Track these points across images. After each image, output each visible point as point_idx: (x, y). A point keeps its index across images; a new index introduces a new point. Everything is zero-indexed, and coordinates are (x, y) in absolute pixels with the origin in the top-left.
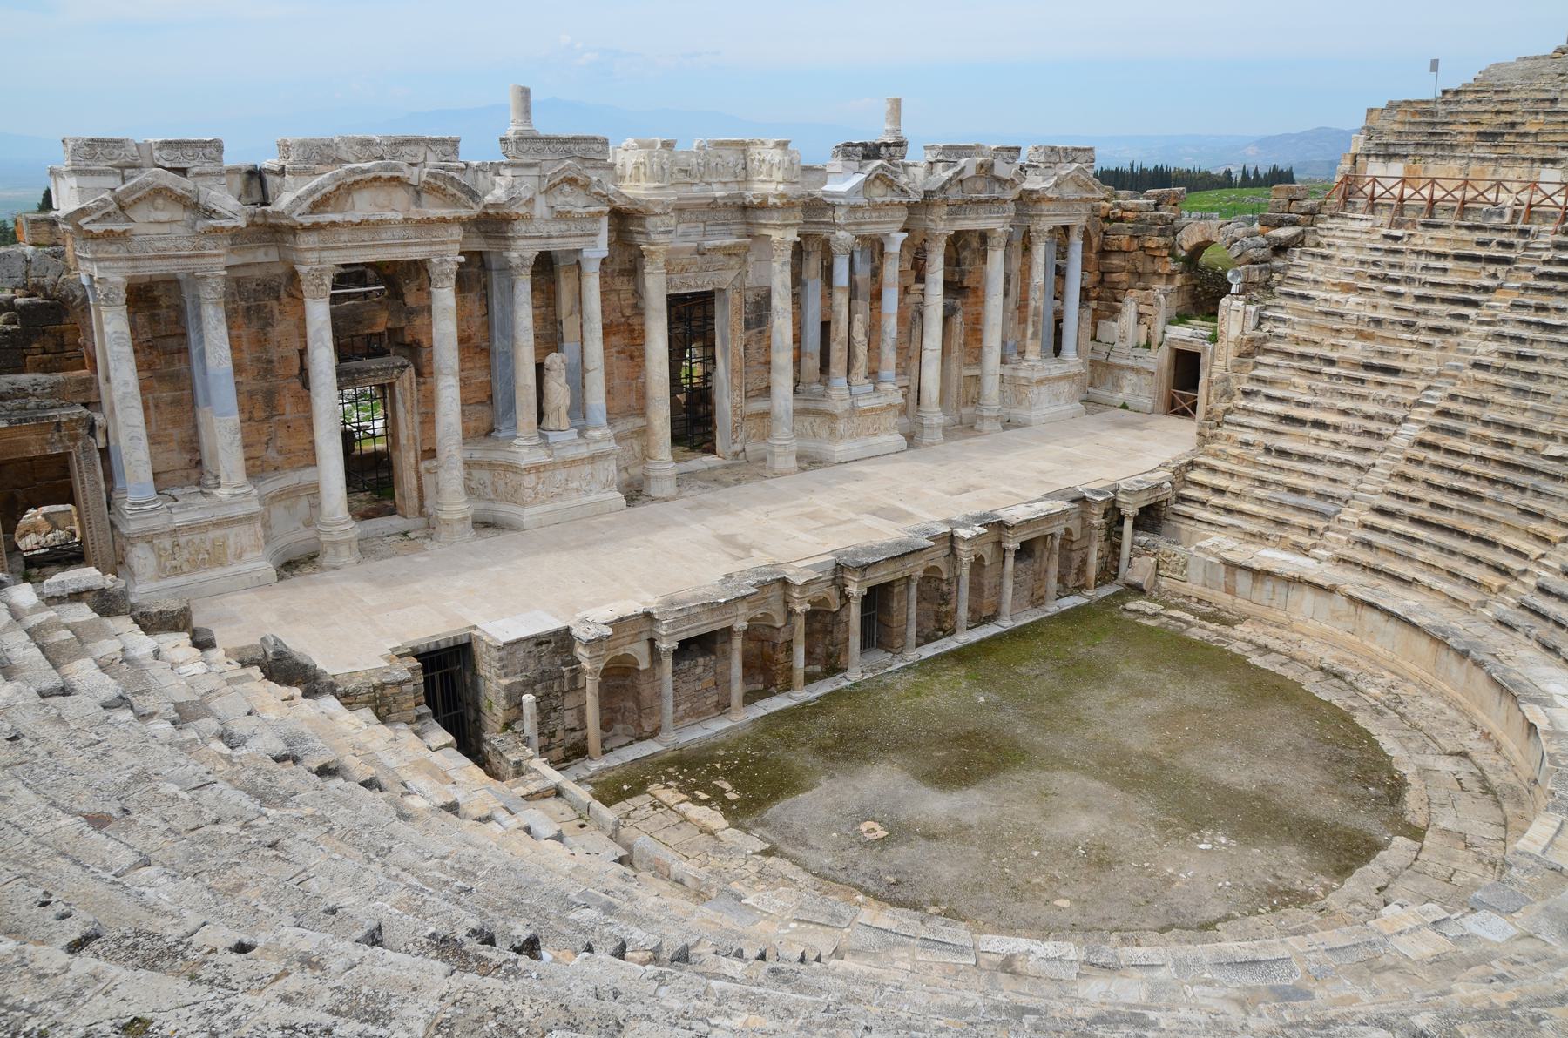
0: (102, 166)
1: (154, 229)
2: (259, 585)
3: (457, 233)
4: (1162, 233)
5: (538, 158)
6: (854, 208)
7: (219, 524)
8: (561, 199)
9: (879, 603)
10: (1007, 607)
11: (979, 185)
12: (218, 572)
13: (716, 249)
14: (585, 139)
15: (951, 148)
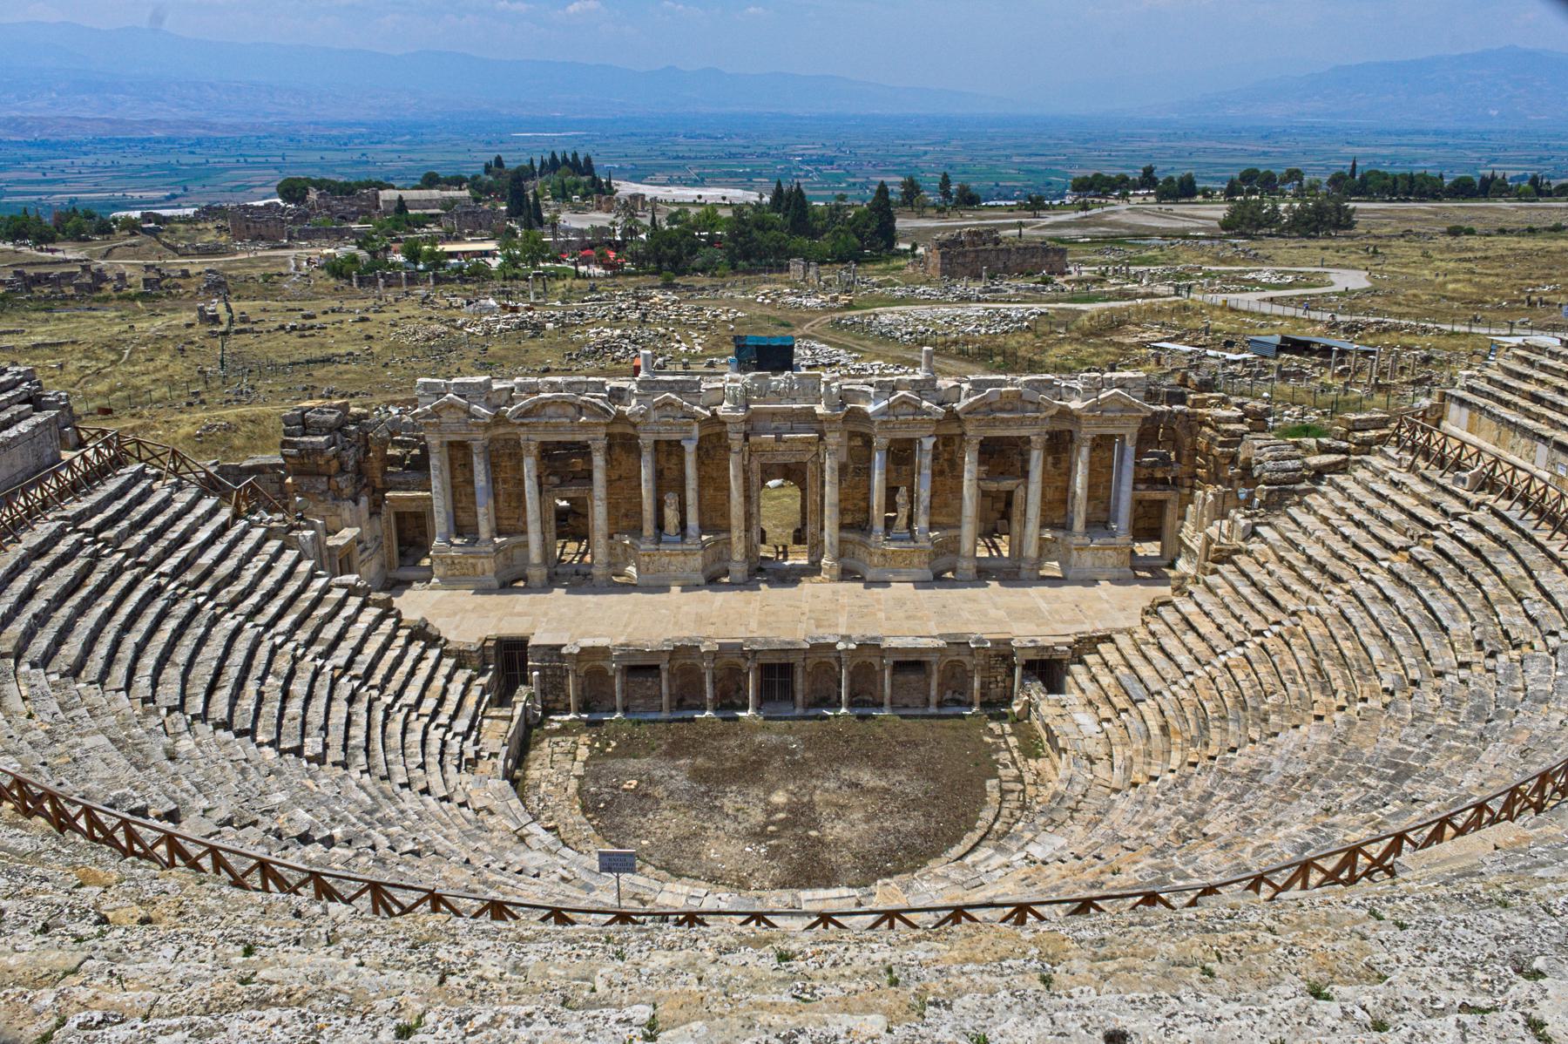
4: (1222, 444)
9: (779, 676)
10: (886, 701)
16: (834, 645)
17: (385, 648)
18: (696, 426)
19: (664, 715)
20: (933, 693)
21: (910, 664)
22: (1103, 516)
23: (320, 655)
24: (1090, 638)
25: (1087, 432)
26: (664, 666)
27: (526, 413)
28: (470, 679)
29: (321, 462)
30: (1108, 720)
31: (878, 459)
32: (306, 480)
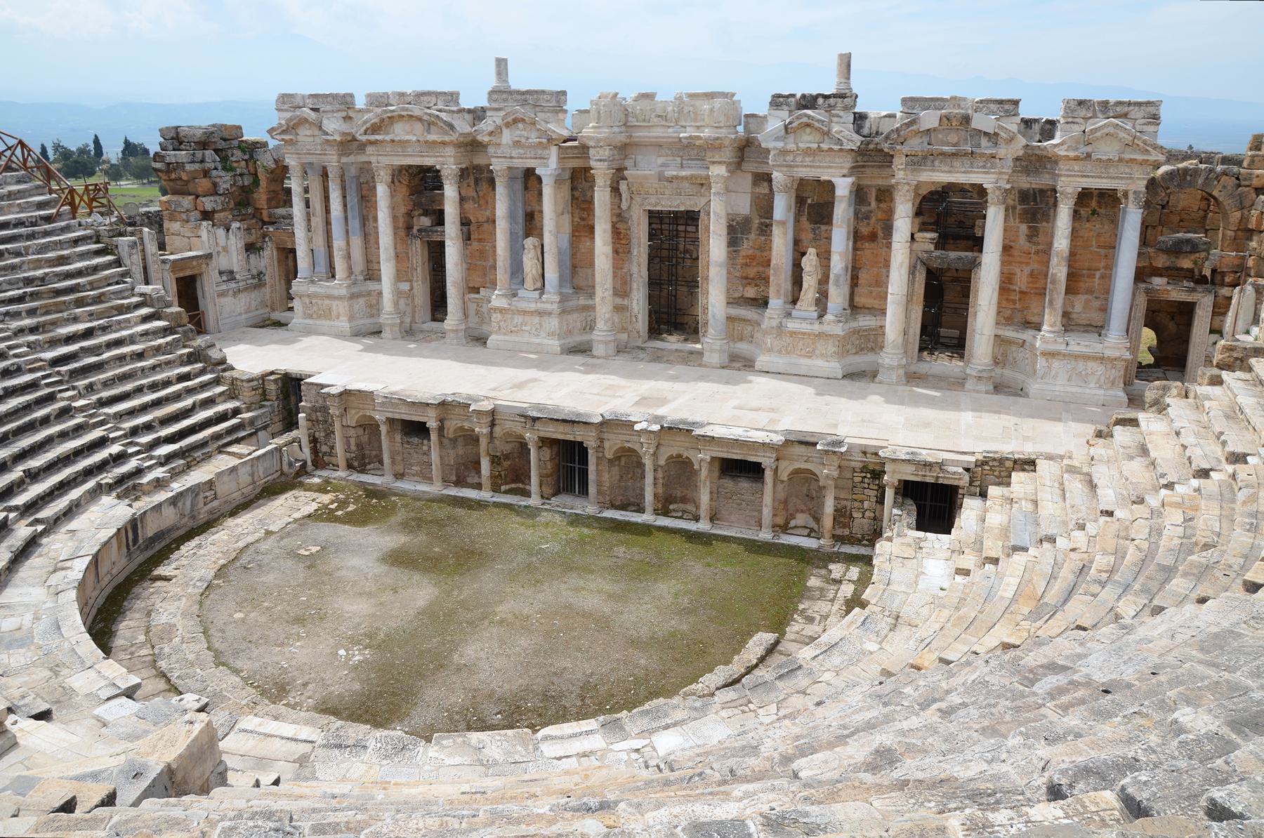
0: (286, 107)
1: (307, 139)
2: (340, 336)
3: (450, 151)
5: (502, 105)
6: (783, 152)
7: (329, 297)
8: (518, 132)
11: (953, 138)
12: (328, 322)
13: (677, 177)
14: (536, 92)
15: (913, 99)
16: (631, 424)
17: (140, 356)
18: (554, 151)
19: (435, 489)
20: (767, 512)
21: (740, 468)
22: (1096, 317)
23: (29, 345)
24: (1002, 461)
25: (1069, 184)
26: (432, 424)
27: (375, 129)
28: (236, 412)
29: (185, 178)
30: (966, 573)
31: (782, 207)
32: (175, 198)
